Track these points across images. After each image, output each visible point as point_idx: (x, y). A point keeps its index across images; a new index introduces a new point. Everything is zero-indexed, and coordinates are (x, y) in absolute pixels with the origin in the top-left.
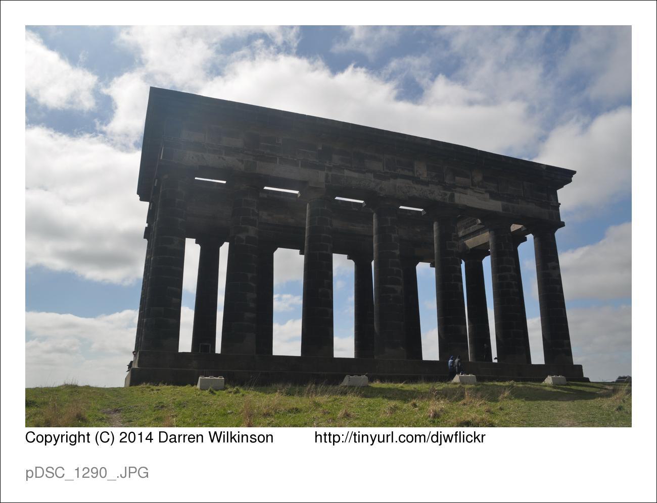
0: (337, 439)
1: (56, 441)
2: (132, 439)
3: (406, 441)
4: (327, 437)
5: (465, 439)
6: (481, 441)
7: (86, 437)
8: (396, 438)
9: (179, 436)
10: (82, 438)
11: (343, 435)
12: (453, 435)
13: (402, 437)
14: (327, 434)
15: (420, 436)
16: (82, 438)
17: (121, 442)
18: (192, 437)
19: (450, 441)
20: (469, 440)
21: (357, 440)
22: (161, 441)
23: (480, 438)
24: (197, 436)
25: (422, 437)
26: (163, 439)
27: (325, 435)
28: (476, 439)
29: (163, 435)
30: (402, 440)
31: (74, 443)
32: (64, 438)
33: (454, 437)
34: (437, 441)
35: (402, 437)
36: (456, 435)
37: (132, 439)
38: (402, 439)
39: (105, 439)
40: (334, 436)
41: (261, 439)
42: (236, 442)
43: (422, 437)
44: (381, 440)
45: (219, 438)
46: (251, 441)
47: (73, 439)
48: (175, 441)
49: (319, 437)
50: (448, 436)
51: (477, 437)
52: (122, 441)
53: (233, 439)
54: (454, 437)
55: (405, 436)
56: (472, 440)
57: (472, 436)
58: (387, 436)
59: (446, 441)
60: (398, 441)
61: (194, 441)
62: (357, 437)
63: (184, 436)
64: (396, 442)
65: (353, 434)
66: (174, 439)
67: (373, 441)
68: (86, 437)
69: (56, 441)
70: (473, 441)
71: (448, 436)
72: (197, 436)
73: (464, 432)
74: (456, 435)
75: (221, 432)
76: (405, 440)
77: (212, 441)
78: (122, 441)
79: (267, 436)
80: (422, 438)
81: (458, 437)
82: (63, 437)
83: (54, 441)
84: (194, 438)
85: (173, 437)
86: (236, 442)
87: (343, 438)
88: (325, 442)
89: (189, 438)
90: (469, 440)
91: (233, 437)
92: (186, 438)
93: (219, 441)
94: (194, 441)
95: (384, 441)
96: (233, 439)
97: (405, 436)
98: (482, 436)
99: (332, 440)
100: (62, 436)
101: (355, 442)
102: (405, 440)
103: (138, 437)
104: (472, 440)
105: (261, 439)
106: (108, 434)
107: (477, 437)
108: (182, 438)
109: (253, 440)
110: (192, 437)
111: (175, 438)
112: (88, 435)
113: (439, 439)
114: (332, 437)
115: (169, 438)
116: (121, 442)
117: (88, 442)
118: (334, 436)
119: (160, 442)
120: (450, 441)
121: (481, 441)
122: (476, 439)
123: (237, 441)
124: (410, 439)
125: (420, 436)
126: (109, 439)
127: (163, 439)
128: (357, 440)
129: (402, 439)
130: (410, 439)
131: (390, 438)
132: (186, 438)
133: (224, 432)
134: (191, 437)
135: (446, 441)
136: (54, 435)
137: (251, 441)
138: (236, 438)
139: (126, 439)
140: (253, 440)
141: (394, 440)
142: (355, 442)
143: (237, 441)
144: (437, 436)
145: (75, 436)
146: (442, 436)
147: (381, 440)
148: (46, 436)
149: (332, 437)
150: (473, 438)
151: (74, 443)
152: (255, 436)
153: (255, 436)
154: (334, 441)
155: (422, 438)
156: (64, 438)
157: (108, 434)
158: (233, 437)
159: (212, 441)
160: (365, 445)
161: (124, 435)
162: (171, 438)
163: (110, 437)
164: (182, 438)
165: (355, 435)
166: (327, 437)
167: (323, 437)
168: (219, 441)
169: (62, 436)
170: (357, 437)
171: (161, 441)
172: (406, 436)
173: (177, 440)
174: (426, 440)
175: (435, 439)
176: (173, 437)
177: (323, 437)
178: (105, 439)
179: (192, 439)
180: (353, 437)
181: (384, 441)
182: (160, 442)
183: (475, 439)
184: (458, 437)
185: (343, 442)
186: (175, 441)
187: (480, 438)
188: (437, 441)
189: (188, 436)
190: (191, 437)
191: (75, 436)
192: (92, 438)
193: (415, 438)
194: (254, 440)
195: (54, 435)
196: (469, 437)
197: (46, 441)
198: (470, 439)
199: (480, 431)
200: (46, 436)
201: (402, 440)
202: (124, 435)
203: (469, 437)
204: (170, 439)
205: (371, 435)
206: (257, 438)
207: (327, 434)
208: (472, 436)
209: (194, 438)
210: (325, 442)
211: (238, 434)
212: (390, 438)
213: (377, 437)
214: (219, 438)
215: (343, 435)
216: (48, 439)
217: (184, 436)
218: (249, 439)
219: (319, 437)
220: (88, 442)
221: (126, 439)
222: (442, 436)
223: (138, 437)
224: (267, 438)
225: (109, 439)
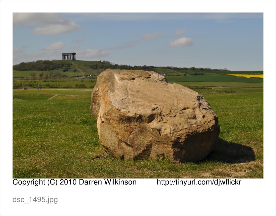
0: (167, 183)
1: (28, 184)
2: (66, 183)
3: (202, 184)
4: (163, 182)
5: (231, 183)
6: (239, 184)
7: (43, 182)
8: (197, 182)
9: (89, 181)
10: (41, 182)
11: (171, 181)
12: (225, 181)
13: (200, 182)
14: (163, 180)
15: (209, 181)
16: (41, 182)
17: (60, 184)
18: (96, 182)
19: (224, 184)
20: (233, 183)
21: (177, 183)
22: (81, 184)
23: (238, 182)
24: (99, 181)
25: (210, 182)
26: (81, 183)
27: (162, 181)
28: (236, 183)
29: (82, 182)
30: (200, 183)
31: (37, 185)
32: (32, 182)
33: (226, 182)
34: (217, 184)
35: (200, 182)
36: (227, 181)
37: (66, 183)
38: (200, 183)
39: (52, 183)
40: (166, 181)
41: (130, 183)
42: (118, 184)
43: (210, 182)
44: (189, 183)
45: (109, 182)
46: (125, 184)
47: (37, 183)
48: (88, 184)
49: (159, 182)
50: (223, 181)
51: (237, 182)
52: (61, 184)
53: (116, 183)
54: (226, 182)
55: (201, 181)
56: (234, 184)
57: (234, 181)
58: (192, 181)
59: (222, 184)
60: (198, 184)
61: (97, 184)
62: (177, 182)
63: (92, 181)
64: (197, 184)
65: (176, 180)
66: (87, 183)
67: (185, 184)
68: (43, 182)
69: (28, 184)
70: (235, 184)
71: (223, 181)
72: (99, 181)
73: (230, 179)
74: (227, 181)
75: (111, 180)
76: (201, 184)
77: (106, 184)
78: (61, 184)
79: (133, 181)
80: (210, 182)
81: (227, 182)
82: (32, 182)
83: (27, 184)
84: (97, 182)
85: (86, 182)
86: (118, 184)
87: (170, 183)
88: (162, 184)
89: (94, 182)
90: (233, 183)
91: (117, 182)
92: (93, 182)
93: (109, 184)
94: (97, 184)
95: (190, 184)
96: (116, 183)
97: (201, 181)
98: (240, 181)
99: (165, 183)
100: (31, 181)
101: (177, 184)
102: (201, 184)
103: (69, 182)
104: (234, 184)
105: (130, 183)
106: (54, 180)
107: (237, 182)
108: (91, 182)
109: (126, 183)
110: (96, 182)
111: (87, 182)
112: (44, 181)
113: (218, 183)
114: (165, 182)
115: (84, 182)
116: (60, 184)
117: (44, 184)
118: (166, 181)
119: (80, 184)
120: (224, 184)
121: (239, 184)
122: (236, 183)
123: (118, 184)
124: (204, 183)
125: (209, 181)
126: (54, 183)
127: (81, 183)
128: (177, 183)
129: (200, 183)
130: (204, 183)
131: (194, 182)
132: (93, 182)
133: (112, 179)
134: (95, 182)
135: (222, 184)
136: (27, 181)
137: (125, 184)
138: (118, 182)
139: (63, 183)
140: (126, 183)
141: (196, 184)
142: (177, 184)
143: (118, 184)
144: (217, 181)
145: (38, 181)
146: (220, 182)
147: (189, 183)
148: (23, 181)
149: (165, 182)
150: (235, 182)
151: (37, 185)
152: (127, 181)
153: (127, 181)
154: (166, 184)
155: (210, 182)
156: (32, 182)
157: (54, 180)
158: (117, 182)
159: (106, 184)
160: (181, 186)
161: (62, 181)
162: (85, 182)
163: (55, 182)
164: (91, 182)
165: (176, 181)
166: (163, 182)
167: (161, 182)
168: (109, 184)
169: (31, 181)
170: (177, 182)
171: (81, 184)
172: (202, 182)
173: (88, 183)
174: (212, 184)
175: (216, 183)
176: (86, 182)
177: (161, 182)
178: (52, 183)
179: (96, 183)
180: (175, 182)
181: (190, 184)
182: (80, 184)
183: (236, 183)
184: (227, 182)
185: (171, 184)
186: (88, 184)
187: (238, 182)
188: (217, 184)
189: (94, 181)
190: (95, 182)
191: (38, 181)
192: (46, 182)
193: (206, 183)
194: (127, 184)
195: (27, 181)
196: (233, 182)
197: (23, 184)
198: (233, 183)
199: (238, 180)
200: (23, 181)
201: (200, 183)
202: (62, 181)
203: (233, 182)
204: (85, 183)
205: (184, 181)
206: (128, 182)
207: (163, 180)
208: (234, 181)
209: (97, 182)
210: (162, 184)
211: (119, 180)
212: (194, 182)
213: (187, 181)
214: (109, 182)
215: (171, 181)
216: (24, 183)
217: (92, 181)
218: (125, 183)
219: (159, 182)
220: (44, 184)
221: (63, 183)
222: (220, 182)
223: (69, 182)
224: (133, 183)
225: (54, 183)
